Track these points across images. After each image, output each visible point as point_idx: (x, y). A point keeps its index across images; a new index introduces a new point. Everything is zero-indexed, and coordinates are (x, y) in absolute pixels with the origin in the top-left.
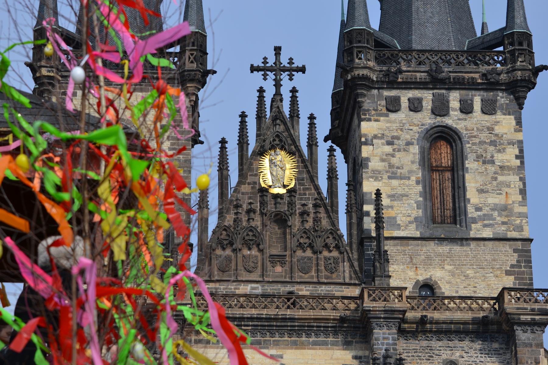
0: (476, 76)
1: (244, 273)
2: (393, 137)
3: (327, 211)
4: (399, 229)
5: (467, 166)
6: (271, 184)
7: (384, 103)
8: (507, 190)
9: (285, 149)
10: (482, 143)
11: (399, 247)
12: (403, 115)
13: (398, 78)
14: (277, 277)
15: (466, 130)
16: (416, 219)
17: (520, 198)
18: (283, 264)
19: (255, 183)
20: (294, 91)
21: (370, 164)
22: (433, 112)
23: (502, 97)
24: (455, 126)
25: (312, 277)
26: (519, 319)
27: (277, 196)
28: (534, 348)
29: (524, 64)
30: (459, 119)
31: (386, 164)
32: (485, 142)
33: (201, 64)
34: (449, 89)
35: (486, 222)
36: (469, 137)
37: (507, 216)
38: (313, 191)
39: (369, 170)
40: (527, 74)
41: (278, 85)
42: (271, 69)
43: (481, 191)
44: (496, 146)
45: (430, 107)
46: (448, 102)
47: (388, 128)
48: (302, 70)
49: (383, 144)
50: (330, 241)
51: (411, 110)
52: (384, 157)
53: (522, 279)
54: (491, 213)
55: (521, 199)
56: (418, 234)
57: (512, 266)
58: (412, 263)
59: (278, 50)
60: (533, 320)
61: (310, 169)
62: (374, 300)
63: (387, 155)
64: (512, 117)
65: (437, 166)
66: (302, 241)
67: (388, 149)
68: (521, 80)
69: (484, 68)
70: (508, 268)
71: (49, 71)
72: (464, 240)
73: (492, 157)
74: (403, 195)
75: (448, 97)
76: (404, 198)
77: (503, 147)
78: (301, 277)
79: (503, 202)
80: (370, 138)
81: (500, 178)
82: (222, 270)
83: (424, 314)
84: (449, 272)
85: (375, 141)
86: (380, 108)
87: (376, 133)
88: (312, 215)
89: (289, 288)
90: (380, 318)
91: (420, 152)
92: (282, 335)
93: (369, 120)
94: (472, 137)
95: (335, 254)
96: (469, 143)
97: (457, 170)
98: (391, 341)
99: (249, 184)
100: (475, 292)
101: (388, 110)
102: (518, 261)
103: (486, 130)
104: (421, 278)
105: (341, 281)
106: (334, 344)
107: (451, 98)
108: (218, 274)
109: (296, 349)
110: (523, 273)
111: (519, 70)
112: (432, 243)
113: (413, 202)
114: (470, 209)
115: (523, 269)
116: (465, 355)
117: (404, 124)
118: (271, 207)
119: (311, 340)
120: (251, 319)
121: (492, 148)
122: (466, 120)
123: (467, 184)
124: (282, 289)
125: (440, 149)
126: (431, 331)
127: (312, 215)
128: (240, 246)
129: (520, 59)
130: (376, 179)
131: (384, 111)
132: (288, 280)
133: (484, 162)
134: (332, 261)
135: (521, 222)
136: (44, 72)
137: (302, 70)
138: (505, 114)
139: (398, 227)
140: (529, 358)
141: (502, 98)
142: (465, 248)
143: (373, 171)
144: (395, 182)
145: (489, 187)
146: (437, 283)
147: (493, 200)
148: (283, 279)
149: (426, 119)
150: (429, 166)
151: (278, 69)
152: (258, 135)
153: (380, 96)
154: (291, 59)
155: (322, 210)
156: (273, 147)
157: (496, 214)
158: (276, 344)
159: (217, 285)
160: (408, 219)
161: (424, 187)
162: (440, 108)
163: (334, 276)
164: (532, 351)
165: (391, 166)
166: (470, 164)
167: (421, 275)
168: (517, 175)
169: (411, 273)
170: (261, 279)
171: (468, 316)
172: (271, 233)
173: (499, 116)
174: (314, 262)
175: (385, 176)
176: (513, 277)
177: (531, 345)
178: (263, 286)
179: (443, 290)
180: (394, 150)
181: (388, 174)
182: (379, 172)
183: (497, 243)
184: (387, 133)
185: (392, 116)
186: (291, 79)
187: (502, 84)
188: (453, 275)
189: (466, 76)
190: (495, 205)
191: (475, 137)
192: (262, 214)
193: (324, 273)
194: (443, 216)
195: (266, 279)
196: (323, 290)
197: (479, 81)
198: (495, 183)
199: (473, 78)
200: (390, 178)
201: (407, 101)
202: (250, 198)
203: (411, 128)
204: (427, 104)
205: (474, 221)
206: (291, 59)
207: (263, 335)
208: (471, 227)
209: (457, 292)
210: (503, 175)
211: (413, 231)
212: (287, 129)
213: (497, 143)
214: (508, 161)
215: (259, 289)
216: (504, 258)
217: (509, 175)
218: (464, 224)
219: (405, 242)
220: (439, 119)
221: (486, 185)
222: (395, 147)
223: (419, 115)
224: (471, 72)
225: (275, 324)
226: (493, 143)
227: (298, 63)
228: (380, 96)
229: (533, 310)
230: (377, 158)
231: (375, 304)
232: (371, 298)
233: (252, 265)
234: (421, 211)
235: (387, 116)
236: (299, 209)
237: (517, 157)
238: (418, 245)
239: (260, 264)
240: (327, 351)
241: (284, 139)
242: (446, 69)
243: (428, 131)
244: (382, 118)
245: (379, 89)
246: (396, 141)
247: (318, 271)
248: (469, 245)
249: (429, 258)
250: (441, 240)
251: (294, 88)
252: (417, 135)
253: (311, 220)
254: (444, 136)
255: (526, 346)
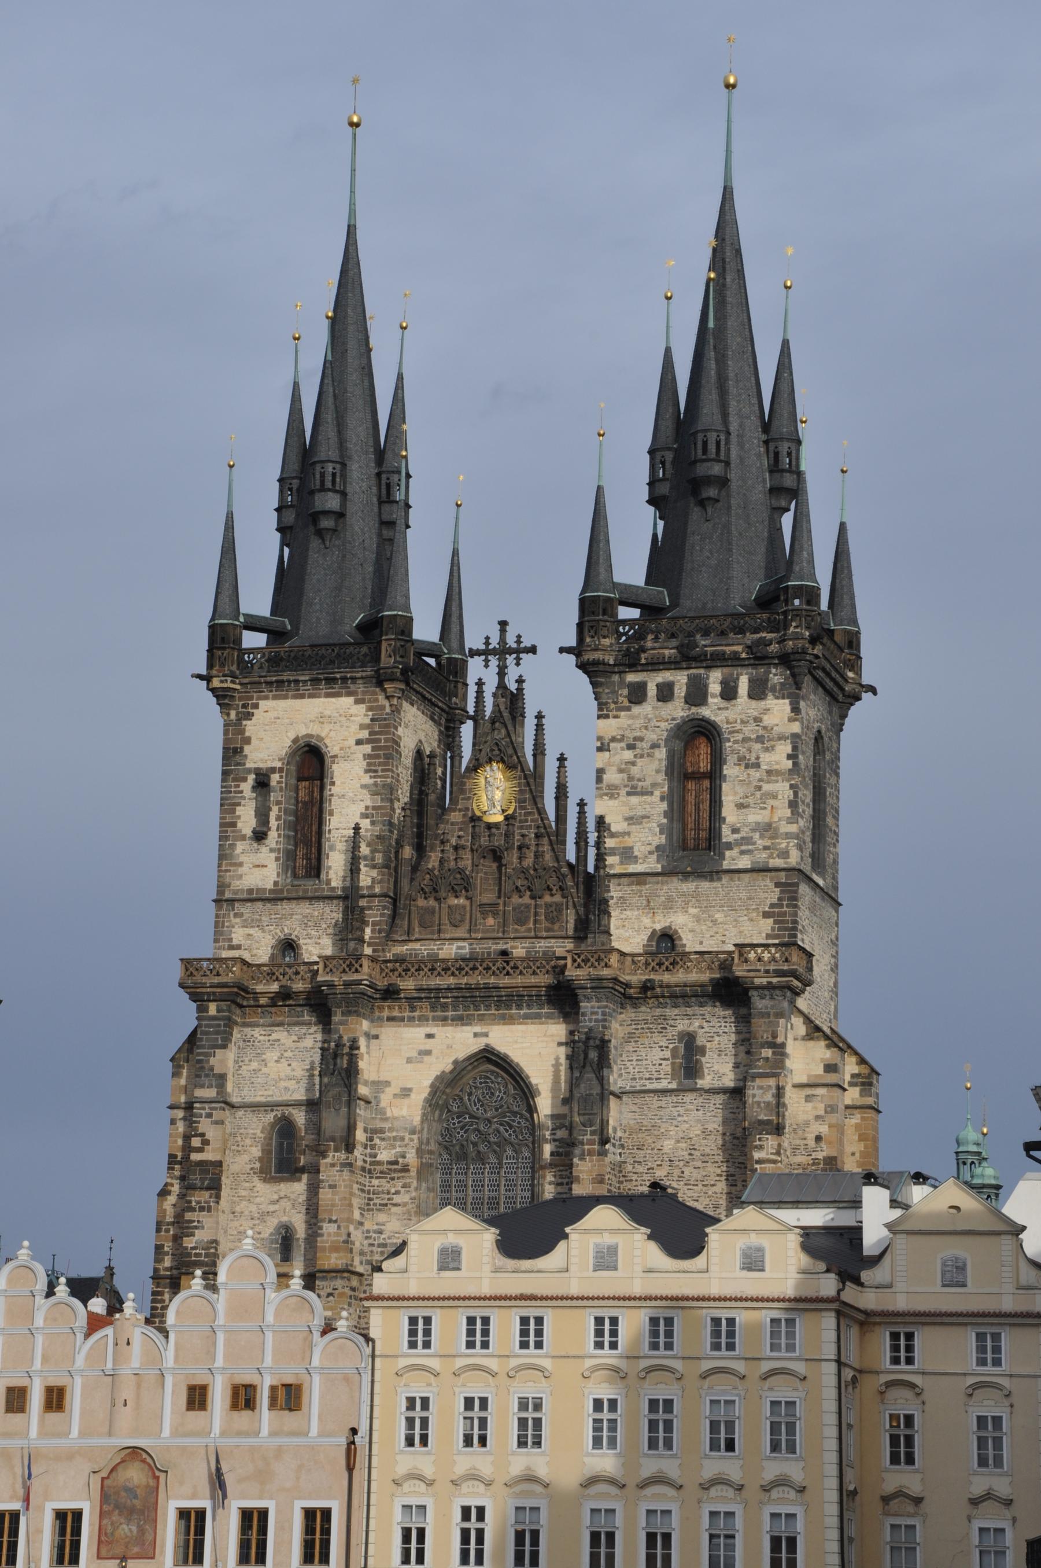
0: (739, 648)
1: (449, 927)
2: (635, 739)
3: (551, 843)
4: (636, 862)
5: (725, 772)
6: (486, 808)
7: (625, 692)
8: (772, 802)
9: (503, 762)
10: (746, 740)
11: (634, 887)
12: (647, 708)
13: (640, 660)
14: (488, 931)
15: (728, 723)
16: (658, 848)
17: (788, 812)
18: (495, 914)
19: (467, 809)
20: (520, 681)
21: (605, 776)
22: (686, 702)
23: (775, 675)
24: (713, 718)
25: (529, 930)
26: (753, 983)
27: (489, 826)
28: (772, 1019)
29: (798, 630)
30: (719, 709)
31: (625, 776)
32: (749, 739)
33: (402, 657)
34: (708, 668)
35: (743, 848)
36: (730, 733)
37: (771, 838)
38: (536, 816)
39: (604, 785)
40: (800, 644)
41: (502, 673)
42: (494, 652)
43: (741, 806)
44: (763, 743)
45: (683, 694)
46: (706, 686)
47: (629, 726)
48: (533, 650)
49: (622, 749)
50: (552, 881)
51: (659, 700)
52: (623, 766)
53: (783, 922)
54: (751, 835)
55: (789, 815)
56: (659, 868)
57: (772, 906)
58: (649, 907)
59: (503, 624)
60: (770, 983)
61: (533, 787)
62: (579, 966)
63: (626, 763)
64: (787, 701)
65: (693, 773)
66: (519, 883)
67: (628, 755)
68: (793, 653)
69: (750, 637)
70: (767, 909)
71: (222, 682)
72: (715, 874)
73: (758, 758)
74: (644, 817)
75: (708, 678)
76: (645, 820)
77: (773, 743)
78: (516, 931)
79: (767, 820)
80: (606, 741)
81: (766, 787)
82: (421, 925)
83: (652, 977)
84: (694, 916)
85: (612, 745)
86: (620, 699)
87: (614, 734)
88: (533, 848)
89: (501, 946)
90: (587, 988)
91: (667, 757)
92: (488, 1007)
93: (607, 717)
94: (734, 732)
95: (558, 898)
96: (729, 741)
97: (714, 776)
98: (600, 1017)
99: (460, 810)
100: (723, 942)
101: (630, 702)
102: (779, 899)
103: (752, 721)
104: (658, 927)
105: (563, 933)
106: (549, 1016)
107: (711, 679)
108: (420, 932)
109: (504, 1024)
110: (784, 914)
111: (791, 639)
112: (675, 879)
113: (655, 825)
114: (725, 831)
115: (785, 909)
116: (705, 1024)
117: (649, 720)
118: (484, 841)
119: (522, 1012)
120: (449, 989)
121: (758, 746)
122: (727, 708)
123: (723, 798)
124: (494, 947)
125: (698, 748)
126: (663, 997)
127: (533, 848)
128: (444, 895)
129: (794, 624)
130: (612, 796)
131: (626, 703)
132: (500, 935)
133: (747, 766)
134: (553, 909)
135: (787, 846)
136: (216, 683)
137: (533, 650)
138: (777, 698)
139: (635, 859)
140: (766, 1031)
141: (776, 677)
142: (715, 884)
143: (609, 787)
144: (634, 800)
145: (750, 800)
146: (676, 932)
147: (755, 817)
148: (495, 935)
149: (677, 710)
150: (681, 773)
151: (503, 651)
152: (474, 745)
153: (622, 684)
154: (519, 636)
155: (545, 841)
156: (490, 761)
157: (756, 836)
158: (481, 1019)
159: (417, 946)
160: (649, 848)
161: (671, 805)
162: (697, 695)
163: (556, 927)
164: (770, 1022)
165: (630, 778)
166: (730, 770)
167: (659, 922)
168: (788, 780)
169: (647, 921)
170: (467, 936)
171: (705, 977)
172: (486, 873)
173: (771, 702)
174: (533, 910)
175: (623, 792)
176: (772, 920)
177: (768, 1015)
178: (471, 944)
179: (684, 942)
180: (635, 756)
181: (627, 789)
182: (616, 787)
183: (755, 875)
184: (628, 733)
185: (636, 710)
186: (518, 664)
187: (773, 658)
188: (698, 919)
189: (728, 649)
190: (758, 824)
191: (737, 732)
192: (472, 850)
193: (544, 924)
194: (697, 839)
195: (473, 935)
196: (542, 945)
197: (744, 655)
198: (758, 793)
199: (736, 653)
200: (629, 794)
201: (655, 688)
202: (461, 829)
203: (658, 724)
204: (680, 691)
205: (729, 846)
206: (519, 636)
207: (466, 1008)
208: (724, 854)
209: (701, 943)
210: (769, 782)
211: (653, 865)
212: (509, 735)
213: (765, 739)
214: (777, 763)
215: (465, 948)
216: (762, 895)
217: (777, 781)
218: (717, 851)
219: (643, 878)
220: (694, 710)
221: (747, 797)
222: (638, 751)
223: (670, 705)
224: (733, 645)
225: (478, 994)
226: (760, 739)
227: (526, 643)
228: (622, 684)
229: (767, 971)
230: (615, 768)
231: (579, 972)
232: (576, 964)
233: (458, 917)
234: (664, 836)
235: (629, 709)
236: (518, 840)
237: (789, 757)
238: (658, 883)
239: (468, 915)
240: (540, 1026)
241: (503, 749)
242: (703, 643)
243: (679, 727)
244: (623, 713)
245: (620, 673)
246: (638, 744)
247: (535, 922)
248: (720, 879)
249: (670, 899)
250: (686, 876)
251: (521, 676)
252: (665, 734)
253: (532, 855)
254: (700, 733)
255: (763, 1017)
